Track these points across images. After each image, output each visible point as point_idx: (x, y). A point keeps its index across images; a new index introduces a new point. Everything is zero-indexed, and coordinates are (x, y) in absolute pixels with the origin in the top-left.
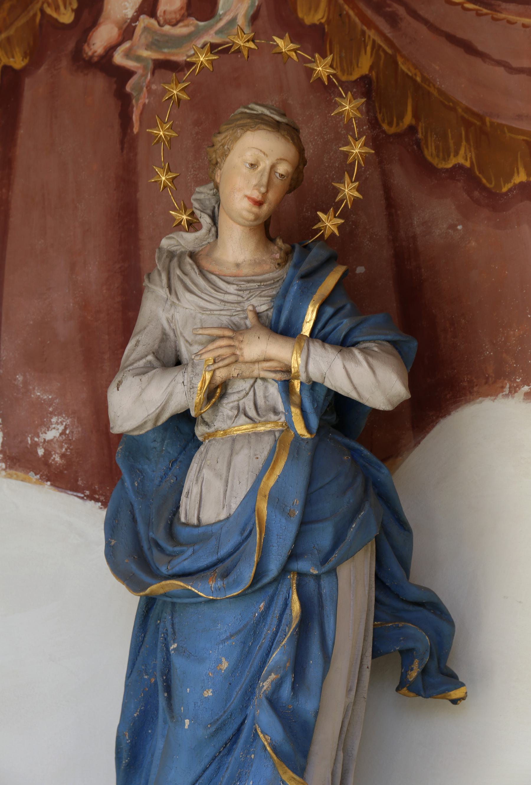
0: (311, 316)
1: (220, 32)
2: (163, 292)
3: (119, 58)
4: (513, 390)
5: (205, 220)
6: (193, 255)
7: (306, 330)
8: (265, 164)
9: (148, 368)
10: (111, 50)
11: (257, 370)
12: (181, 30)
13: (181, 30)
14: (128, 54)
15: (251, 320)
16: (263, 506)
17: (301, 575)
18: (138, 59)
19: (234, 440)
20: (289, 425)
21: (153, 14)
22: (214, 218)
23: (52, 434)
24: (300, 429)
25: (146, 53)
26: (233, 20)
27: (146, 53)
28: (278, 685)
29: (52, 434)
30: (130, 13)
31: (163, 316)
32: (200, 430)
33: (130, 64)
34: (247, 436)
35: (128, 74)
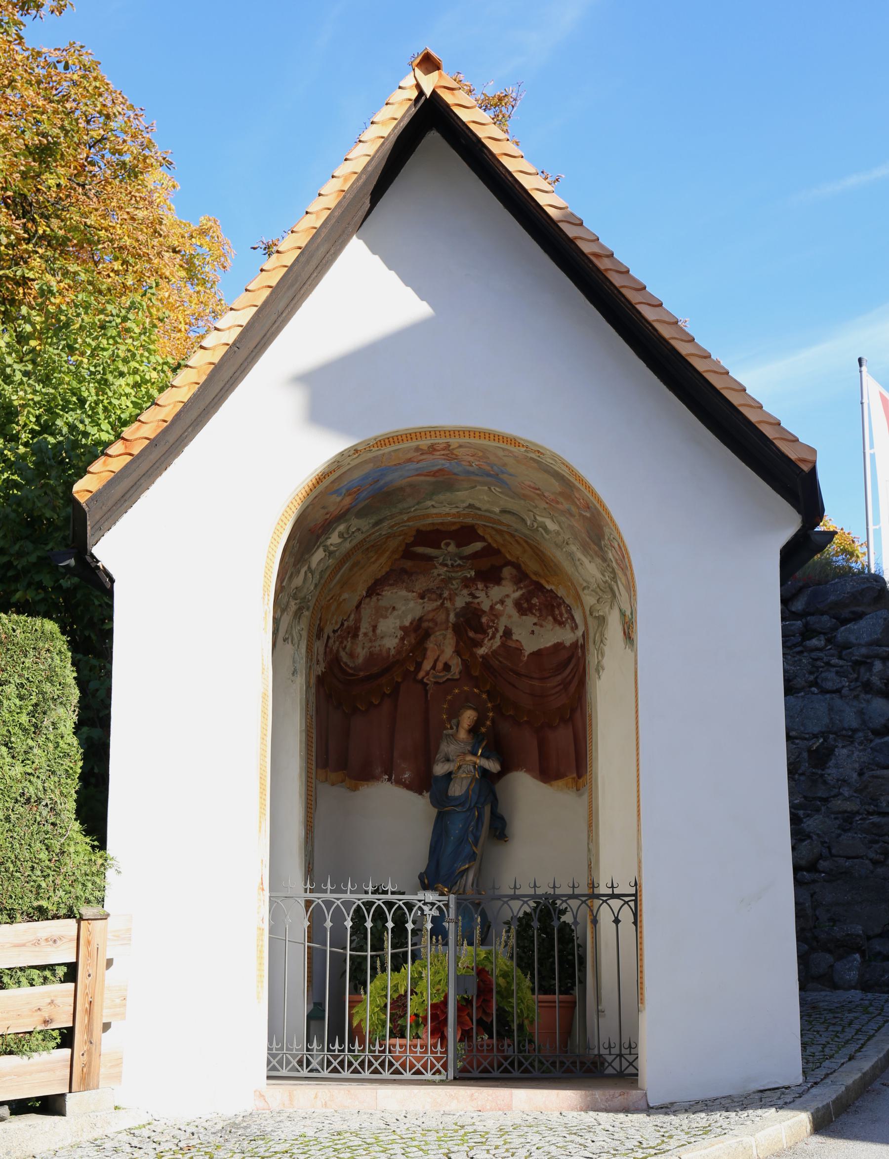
0: (480, 751)
1: (452, 675)
2: (445, 744)
3: (425, 680)
4: (522, 770)
5: (455, 727)
6: (452, 735)
7: (479, 754)
8: (472, 717)
9: (443, 762)
10: (423, 678)
11: (468, 763)
12: (441, 674)
13: (441, 674)
14: (428, 679)
15: (467, 752)
16: (470, 792)
17: (477, 807)
18: (430, 681)
19: (462, 778)
20: (475, 775)
21: (434, 669)
22: (458, 727)
23: (406, 776)
24: (477, 776)
25: (432, 680)
26: (455, 673)
27: (432, 680)
28: (473, 829)
29: (406, 776)
30: (428, 669)
31: (446, 750)
32: (453, 776)
33: (428, 682)
34: (465, 777)
35: (427, 684)
